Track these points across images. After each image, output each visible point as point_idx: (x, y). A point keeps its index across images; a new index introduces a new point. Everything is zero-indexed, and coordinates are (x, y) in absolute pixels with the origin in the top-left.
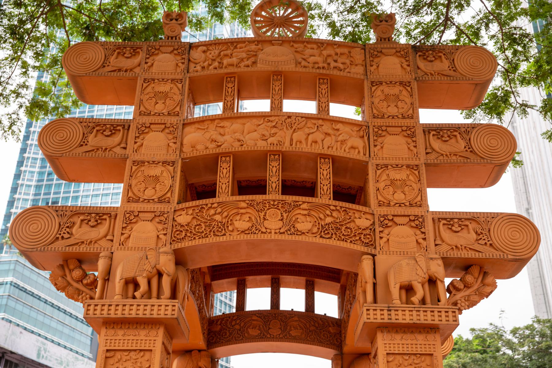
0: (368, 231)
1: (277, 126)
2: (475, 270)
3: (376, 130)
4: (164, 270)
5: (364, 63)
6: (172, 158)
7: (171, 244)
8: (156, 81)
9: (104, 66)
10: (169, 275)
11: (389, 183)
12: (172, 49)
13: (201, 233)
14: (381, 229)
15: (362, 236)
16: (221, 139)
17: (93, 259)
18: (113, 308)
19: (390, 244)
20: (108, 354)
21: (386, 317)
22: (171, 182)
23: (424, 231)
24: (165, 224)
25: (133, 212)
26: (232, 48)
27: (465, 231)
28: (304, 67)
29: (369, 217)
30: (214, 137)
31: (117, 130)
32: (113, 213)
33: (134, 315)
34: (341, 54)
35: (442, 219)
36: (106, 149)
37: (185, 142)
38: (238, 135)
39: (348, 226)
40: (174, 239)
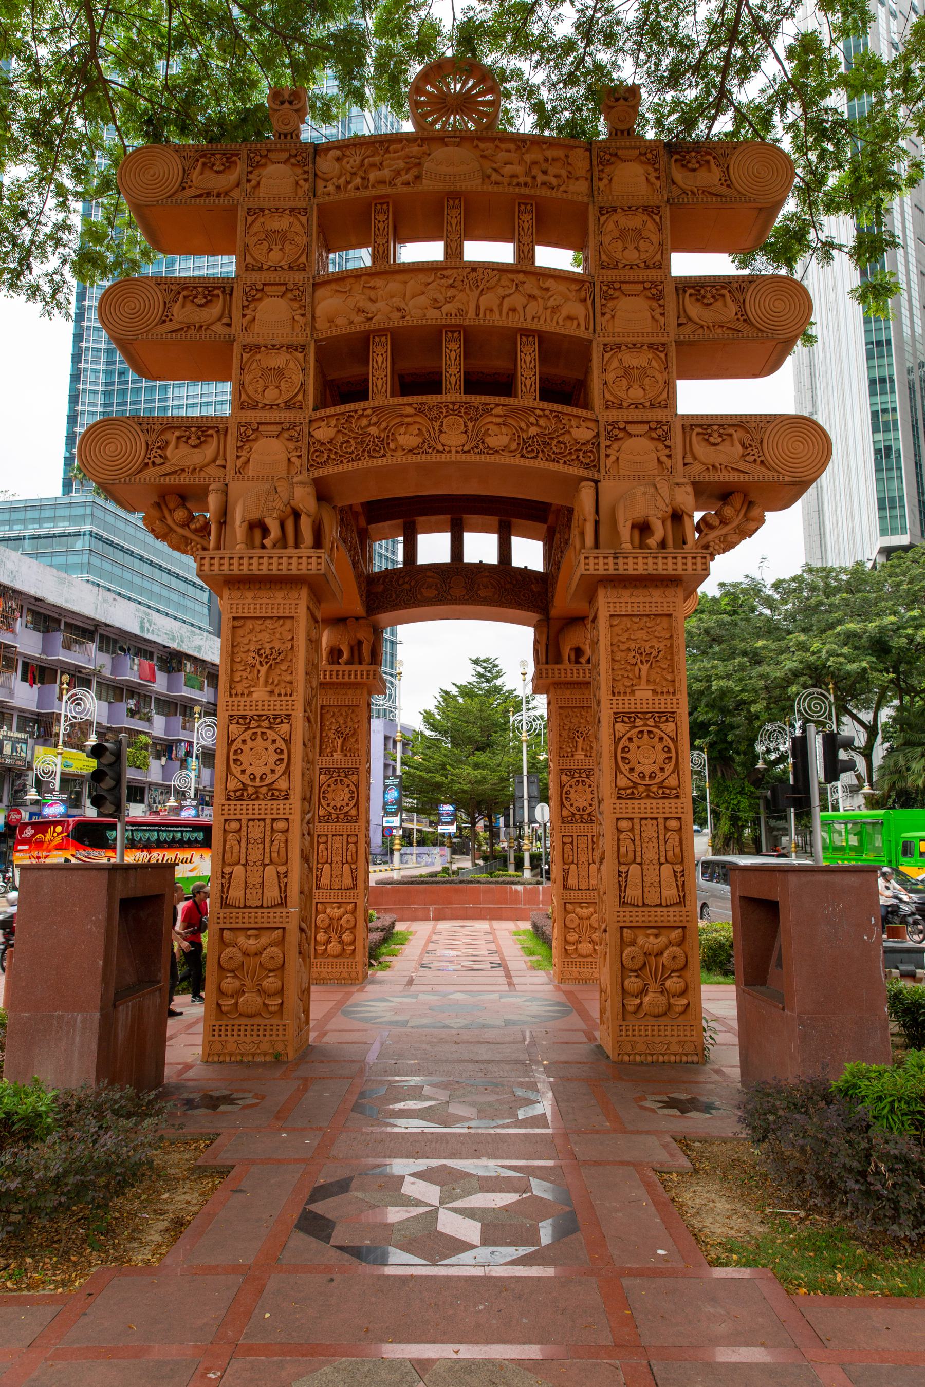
0: (589, 447)
1: (455, 284)
2: (737, 500)
3: (605, 288)
5: (589, 176)
6: (299, 339)
8: (267, 212)
9: (184, 188)
10: (309, 516)
11: (621, 372)
12: (286, 155)
14: (608, 443)
15: (581, 454)
16: (372, 308)
17: (201, 494)
18: (235, 561)
20: (236, 623)
21: (611, 566)
22: (300, 376)
25: (250, 424)
26: (382, 152)
27: (727, 443)
28: (497, 183)
29: (591, 425)
30: (361, 304)
31: (213, 296)
32: (221, 426)
33: (265, 572)
34: (553, 160)
35: (697, 426)
36: (201, 327)
37: (318, 313)
38: (397, 301)
39: (561, 439)
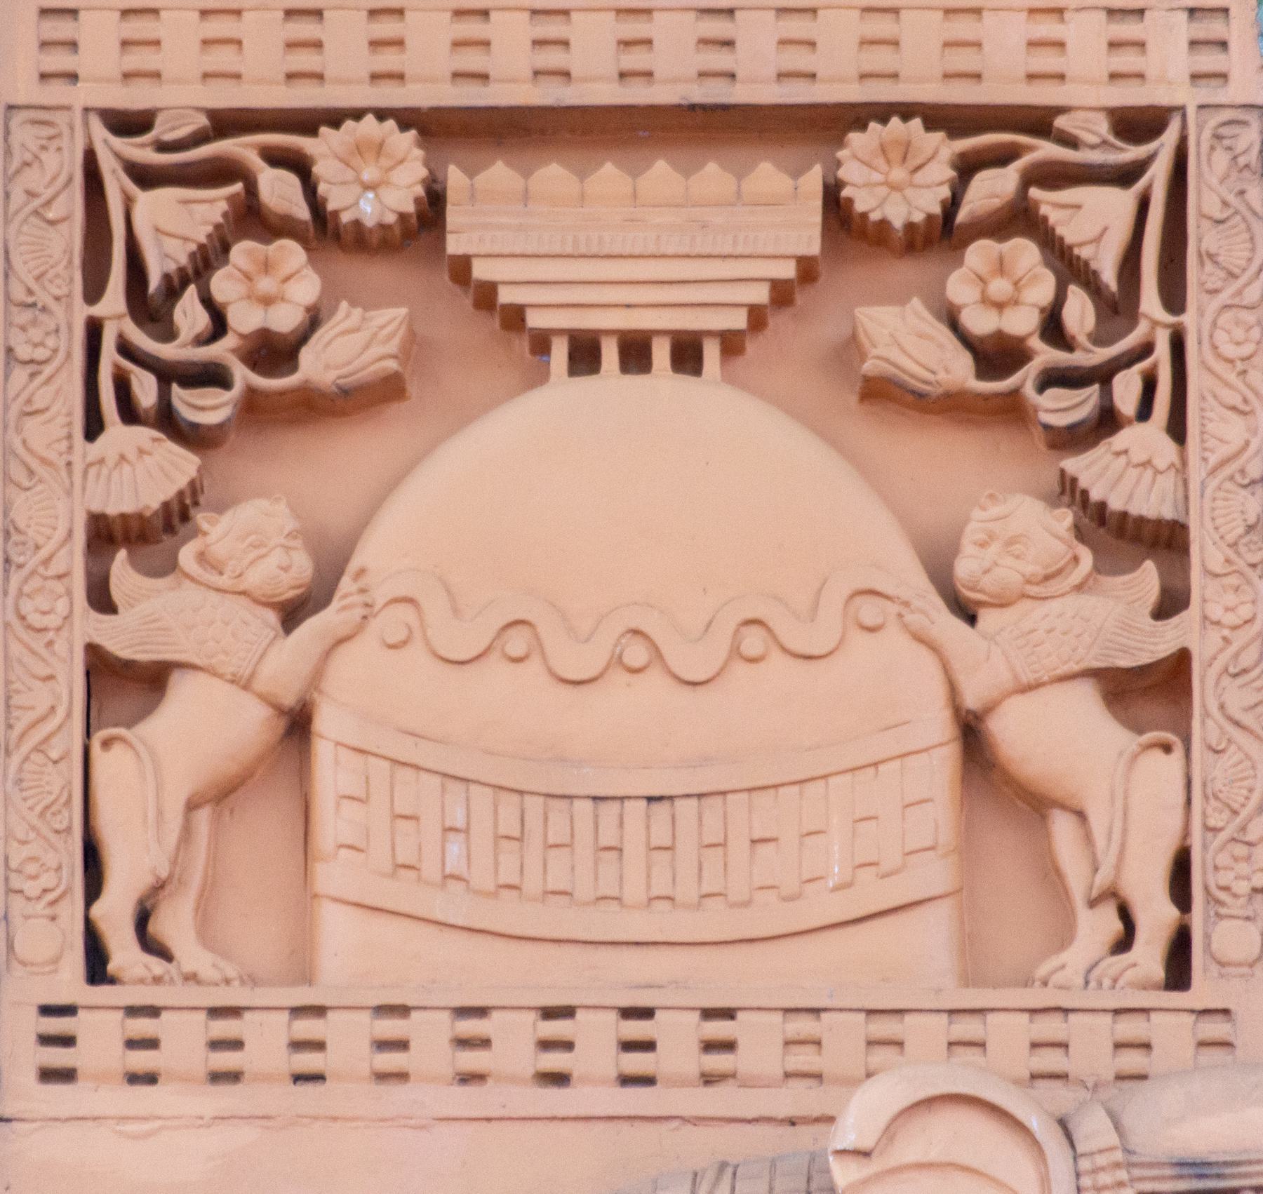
14: (141, 470)
19: (333, 823)
23: (1149, 500)
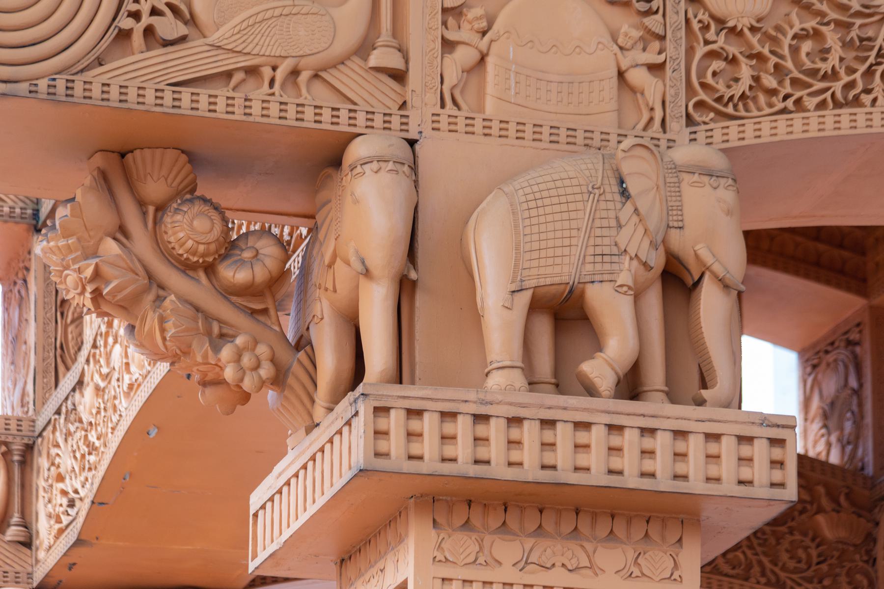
4: (708, 259)
7: (690, 121)
10: (726, 286)
13: (825, 77)
18: (495, 430)
24: (649, 13)
33: (597, 477)
40: (702, 96)
